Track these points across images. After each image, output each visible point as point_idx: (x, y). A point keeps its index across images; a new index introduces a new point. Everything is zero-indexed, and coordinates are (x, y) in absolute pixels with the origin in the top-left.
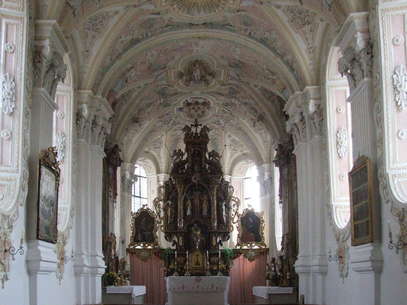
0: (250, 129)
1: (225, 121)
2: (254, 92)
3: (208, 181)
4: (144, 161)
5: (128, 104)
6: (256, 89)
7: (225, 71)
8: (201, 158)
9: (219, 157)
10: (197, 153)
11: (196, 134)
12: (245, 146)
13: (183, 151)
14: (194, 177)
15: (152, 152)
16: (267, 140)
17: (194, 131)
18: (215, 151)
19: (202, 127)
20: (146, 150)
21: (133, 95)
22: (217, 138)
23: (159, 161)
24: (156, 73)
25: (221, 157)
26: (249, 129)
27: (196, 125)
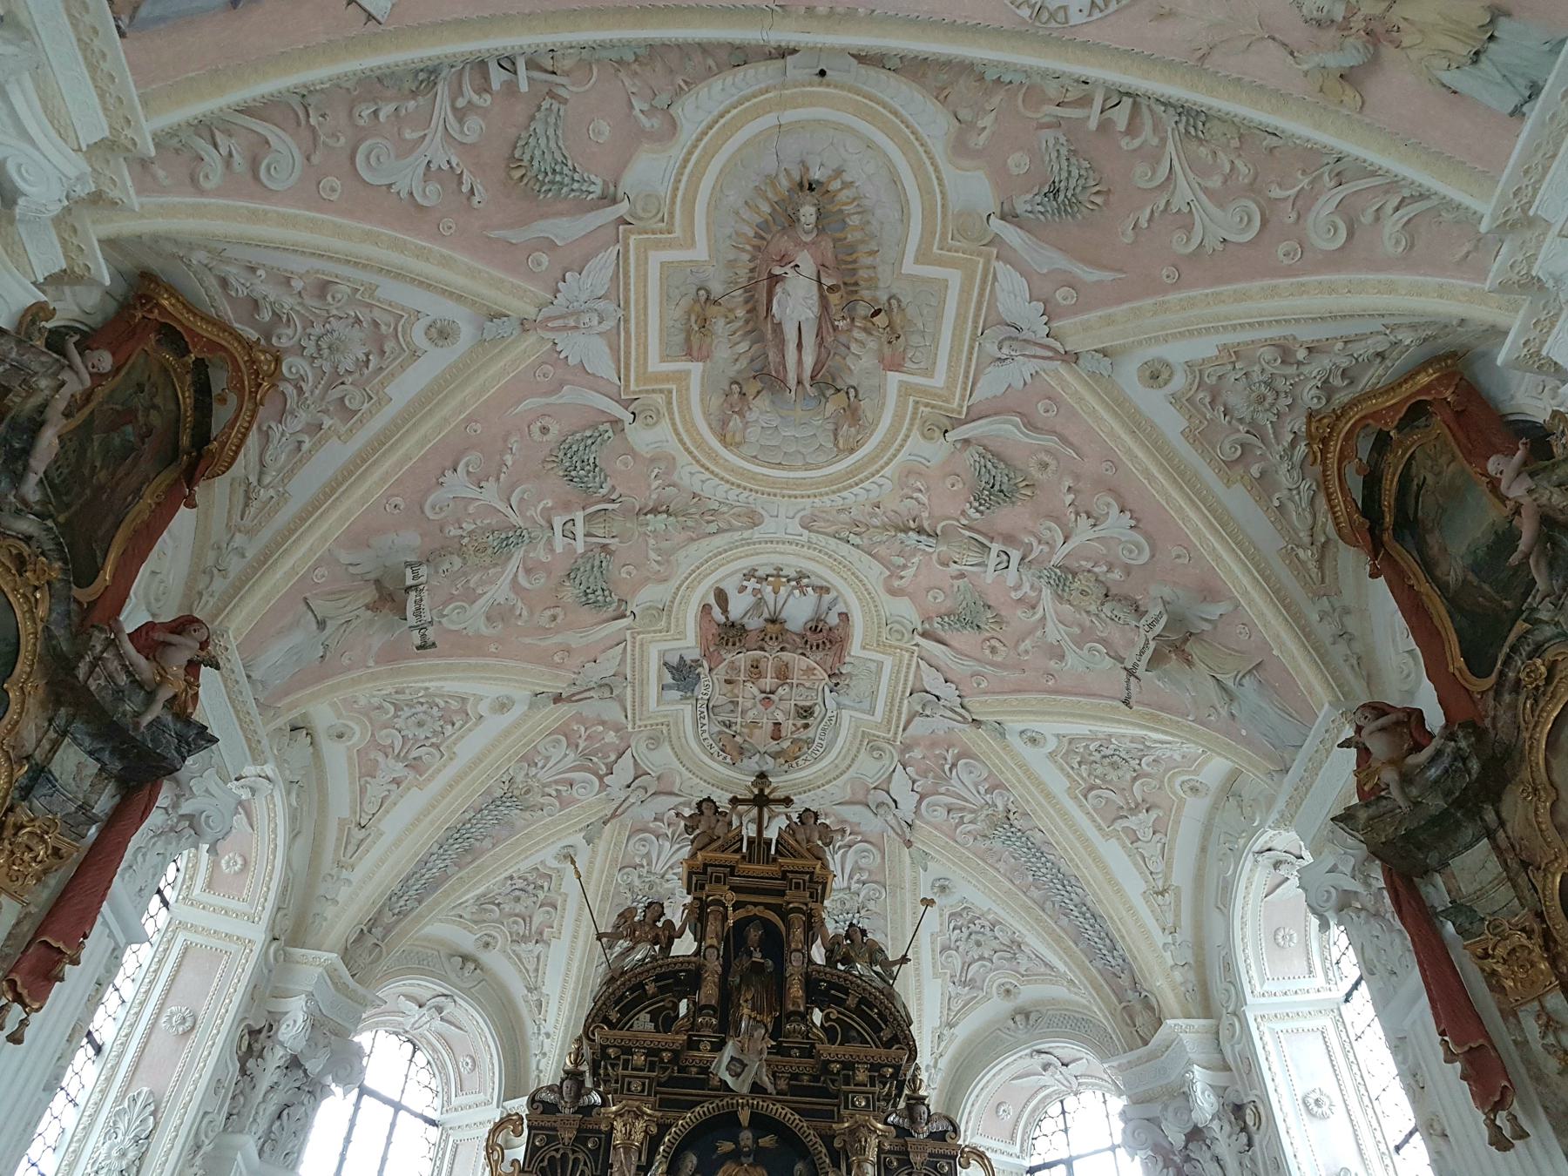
2: (1138, 424)
3: (821, 1089)
4: (440, 1009)
8: (780, 962)
9: (887, 965)
10: (754, 934)
11: (759, 843)
12: (1034, 942)
13: (675, 914)
14: (729, 1050)
16: (1175, 880)
17: (750, 831)
18: (864, 932)
20: (467, 941)
21: (405, 387)
22: (871, 905)
23: (531, 1028)
24: (565, 229)
26: (1064, 814)
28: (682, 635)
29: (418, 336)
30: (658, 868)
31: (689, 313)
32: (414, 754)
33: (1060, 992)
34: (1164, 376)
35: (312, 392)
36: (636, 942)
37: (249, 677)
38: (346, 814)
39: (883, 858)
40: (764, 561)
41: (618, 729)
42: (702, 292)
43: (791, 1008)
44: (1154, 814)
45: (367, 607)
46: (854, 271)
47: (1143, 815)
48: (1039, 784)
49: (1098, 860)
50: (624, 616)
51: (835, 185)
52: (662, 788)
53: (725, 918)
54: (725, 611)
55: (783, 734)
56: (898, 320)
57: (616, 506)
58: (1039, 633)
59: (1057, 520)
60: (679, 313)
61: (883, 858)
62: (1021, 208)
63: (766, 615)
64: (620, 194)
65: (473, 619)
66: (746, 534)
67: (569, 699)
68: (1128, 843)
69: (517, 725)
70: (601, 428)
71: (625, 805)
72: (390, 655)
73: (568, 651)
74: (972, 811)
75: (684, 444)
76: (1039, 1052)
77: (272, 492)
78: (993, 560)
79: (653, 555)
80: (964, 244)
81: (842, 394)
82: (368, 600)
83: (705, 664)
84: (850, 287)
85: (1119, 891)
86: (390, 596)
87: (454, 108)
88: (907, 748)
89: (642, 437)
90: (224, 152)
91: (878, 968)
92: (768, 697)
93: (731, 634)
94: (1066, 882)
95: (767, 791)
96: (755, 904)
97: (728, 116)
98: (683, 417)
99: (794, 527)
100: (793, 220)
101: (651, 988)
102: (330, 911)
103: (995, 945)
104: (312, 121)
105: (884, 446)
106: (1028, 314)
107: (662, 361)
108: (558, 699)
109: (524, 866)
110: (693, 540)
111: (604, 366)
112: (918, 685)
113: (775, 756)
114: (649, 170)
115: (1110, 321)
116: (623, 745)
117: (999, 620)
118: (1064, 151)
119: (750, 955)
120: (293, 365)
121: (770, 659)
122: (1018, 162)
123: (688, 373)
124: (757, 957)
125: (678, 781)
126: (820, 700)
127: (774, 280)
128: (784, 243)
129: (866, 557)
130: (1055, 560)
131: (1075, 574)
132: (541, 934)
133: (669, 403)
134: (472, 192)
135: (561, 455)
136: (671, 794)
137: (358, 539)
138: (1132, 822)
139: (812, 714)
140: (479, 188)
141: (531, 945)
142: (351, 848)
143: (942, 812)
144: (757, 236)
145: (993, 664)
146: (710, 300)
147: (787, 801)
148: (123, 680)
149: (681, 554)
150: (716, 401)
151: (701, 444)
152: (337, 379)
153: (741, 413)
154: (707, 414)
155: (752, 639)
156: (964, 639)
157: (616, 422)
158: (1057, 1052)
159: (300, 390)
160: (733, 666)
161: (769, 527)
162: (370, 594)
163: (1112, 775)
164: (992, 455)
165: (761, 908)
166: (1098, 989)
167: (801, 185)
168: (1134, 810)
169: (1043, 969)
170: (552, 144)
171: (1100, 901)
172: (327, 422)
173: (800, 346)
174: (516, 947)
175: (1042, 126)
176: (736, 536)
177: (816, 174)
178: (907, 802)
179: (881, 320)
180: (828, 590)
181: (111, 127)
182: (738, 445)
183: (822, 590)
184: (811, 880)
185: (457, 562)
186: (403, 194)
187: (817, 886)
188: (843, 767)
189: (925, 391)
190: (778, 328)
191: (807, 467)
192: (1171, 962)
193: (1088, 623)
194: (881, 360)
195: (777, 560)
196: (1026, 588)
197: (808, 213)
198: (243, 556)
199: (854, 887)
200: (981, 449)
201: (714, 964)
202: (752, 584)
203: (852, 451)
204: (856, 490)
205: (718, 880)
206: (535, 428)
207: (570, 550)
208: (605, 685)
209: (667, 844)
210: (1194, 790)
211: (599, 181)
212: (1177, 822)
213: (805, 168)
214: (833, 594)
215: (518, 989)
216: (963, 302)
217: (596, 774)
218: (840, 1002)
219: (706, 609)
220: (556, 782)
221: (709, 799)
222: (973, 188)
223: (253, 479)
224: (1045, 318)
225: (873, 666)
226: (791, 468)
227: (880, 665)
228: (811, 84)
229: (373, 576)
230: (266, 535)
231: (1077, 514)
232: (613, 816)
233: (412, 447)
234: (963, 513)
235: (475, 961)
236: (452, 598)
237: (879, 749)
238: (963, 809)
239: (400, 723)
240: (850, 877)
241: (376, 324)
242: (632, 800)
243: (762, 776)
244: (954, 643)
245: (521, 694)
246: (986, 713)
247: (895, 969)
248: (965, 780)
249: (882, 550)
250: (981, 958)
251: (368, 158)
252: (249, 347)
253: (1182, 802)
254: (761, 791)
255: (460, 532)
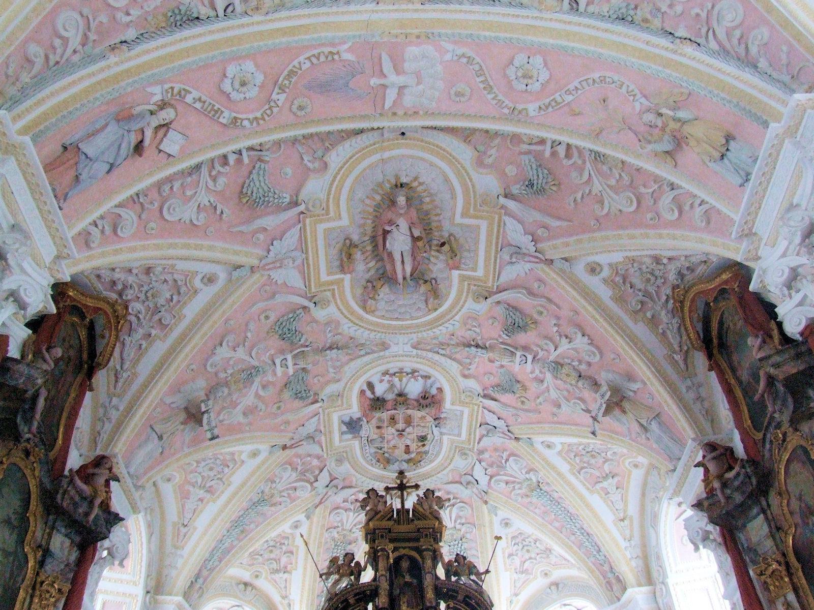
0: (572, 479)
1: (490, 471)
5: (170, 340)
6: (595, 283)
7: (490, 225)
9: (478, 574)
10: (405, 564)
11: (403, 511)
12: (558, 549)
15: (263, 584)
17: (397, 505)
18: (465, 558)
19: (421, 492)
20: (246, 576)
21: (191, 310)
22: (468, 536)
24: (270, 221)
25: (487, 572)
26: (569, 484)
27: (402, 487)
28: (350, 407)
29: (197, 283)
30: (348, 527)
31: (341, 251)
32: (208, 485)
33: (574, 572)
34: (598, 270)
35: (144, 319)
36: (342, 576)
37: (128, 473)
38: (175, 519)
39: (472, 510)
40: (393, 367)
41: (318, 457)
42: (347, 241)
43: (428, 604)
44: (616, 479)
45: (182, 423)
46: (429, 224)
47: (610, 480)
48: (554, 468)
49: (588, 505)
50: (316, 401)
51: (415, 184)
52: (347, 483)
53: (388, 557)
54: (373, 393)
55: (411, 450)
56: (455, 246)
57: (309, 349)
58: (546, 394)
59: (551, 340)
60: (334, 252)
61: (472, 510)
62: (515, 190)
63: (396, 392)
64: (300, 201)
65: (237, 416)
66: (382, 354)
67: (291, 447)
68: (603, 495)
69: (263, 463)
70: (298, 312)
71: (326, 497)
72: (196, 442)
73: (287, 423)
74: (519, 483)
75: (342, 313)
76: (565, 605)
77: (129, 373)
78: (518, 359)
79: (331, 370)
80: (486, 208)
81: (428, 283)
82: (181, 419)
83: (364, 419)
84: (428, 230)
85: (600, 521)
86: (194, 415)
87: (210, 175)
88: (481, 452)
89: (320, 314)
90: (100, 227)
91: (473, 577)
92: (401, 433)
93: (378, 403)
94: (572, 517)
95: (404, 482)
96: (404, 548)
97: (354, 158)
98: (342, 300)
99: (408, 348)
100: (393, 203)
101: (352, 601)
102: (174, 573)
103: (537, 551)
104: (141, 200)
105: (453, 306)
106: (525, 241)
107: (328, 275)
108: (284, 447)
109: (273, 534)
110: (352, 360)
111: (297, 282)
112: (483, 421)
113: (408, 461)
114: (314, 188)
115: (567, 245)
116: (322, 465)
117: (525, 388)
118: (534, 166)
119: (404, 577)
120: (135, 307)
121: (400, 413)
122: (511, 171)
123: (343, 280)
124: (408, 578)
125: (354, 480)
126: (430, 432)
127: (386, 233)
128: (390, 215)
129: (449, 361)
130: (552, 358)
131: (562, 365)
132: (286, 567)
133: (333, 295)
134: (222, 212)
135: (277, 329)
136: (350, 487)
137: (176, 389)
138: (605, 484)
139: (426, 439)
140: (226, 210)
141: (281, 575)
142: (181, 538)
143: (503, 485)
144: (375, 210)
145: (523, 410)
146: (352, 245)
147: (417, 487)
148: (77, 498)
149: (346, 368)
150: (359, 291)
151: (353, 313)
152: (157, 310)
153: (373, 298)
154: (354, 297)
155: (389, 405)
156: (506, 398)
157: (305, 308)
158: (574, 604)
159: (139, 318)
160: (380, 420)
161: (394, 349)
162: (183, 416)
163: (593, 461)
164: (512, 308)
165: (407, 550)
166: (592, 572)
167: (396, 186)
168: (606, 477)
169: (564, 562)
170: (262, 184)
171: (590, 527)
172: (154, 332)
173: (403, 262)
174: (273, 576)
175: (521, 153)
176: (376, 355)
177: (404, 180)
178: (483, 480)
179: (446, 248)
180: (429, 377)
181: (58, 250)
182: (373, 311)
183: (426, 377)
184: (433, 531)
185: (226, 390)
186: (187, 222)
187: (436, 534)
188: (446, 465)
189: (474, 279)
190: (390, 255)
191: (412, 318)
192: (629, 556)
193: (572, 390)
194: (448, 265)
195: (400, 365)
196: (537, 372)
197: (401, 200)
198: (118, 410)
199: (458, 527)
200: (506, 306)
201: (384, 585)
202: (387, 378)
203: (436, 310)
204: (440, 328)
205: (382, 537)
206: (262, 317)
207: (285, 374)
208: (310, 438)
209: (351, 514)
210: (636, 466)
211: (288, 196)
212: (628, 482)
213: (397, 177)
214: (432, 379)
215: (276, 598)
216: (489, 235)
217: (308, 481)
218: (453, 598)
219: (362, 392)
220: (287, 489)
221: (373, 489)
222: (488, 182)
223: (118, 367)
224: (533, 243)
225: (458, 413)
226: (403, 320)
227: (462, 412)
228: (397, 140)
229: (183, 406)
230: (128, 397)
231: (560, 336)
232: (320, 503)
233: (197, 341)
234: (500, 336)
235: (251, 585)
236: (223, 408)
237: (465, 454)
238: (514, 482)
239: (200, 470)
240: (455, 521)
241: (175, 281)
242: (329, 493)
243: (401, 473)
244: (502, 400)
245: (264, 447)
246: (521, 434)
247: (483, 576)
248: (513, 467)
249: (458, 356)
250: (530, 558)
251: (169, 209)
252: (113, 305)
253: (630, 472)
254: (402, 482)
255: (225, 375)
